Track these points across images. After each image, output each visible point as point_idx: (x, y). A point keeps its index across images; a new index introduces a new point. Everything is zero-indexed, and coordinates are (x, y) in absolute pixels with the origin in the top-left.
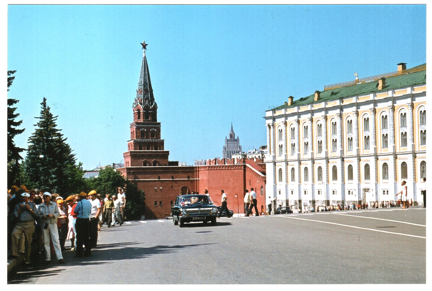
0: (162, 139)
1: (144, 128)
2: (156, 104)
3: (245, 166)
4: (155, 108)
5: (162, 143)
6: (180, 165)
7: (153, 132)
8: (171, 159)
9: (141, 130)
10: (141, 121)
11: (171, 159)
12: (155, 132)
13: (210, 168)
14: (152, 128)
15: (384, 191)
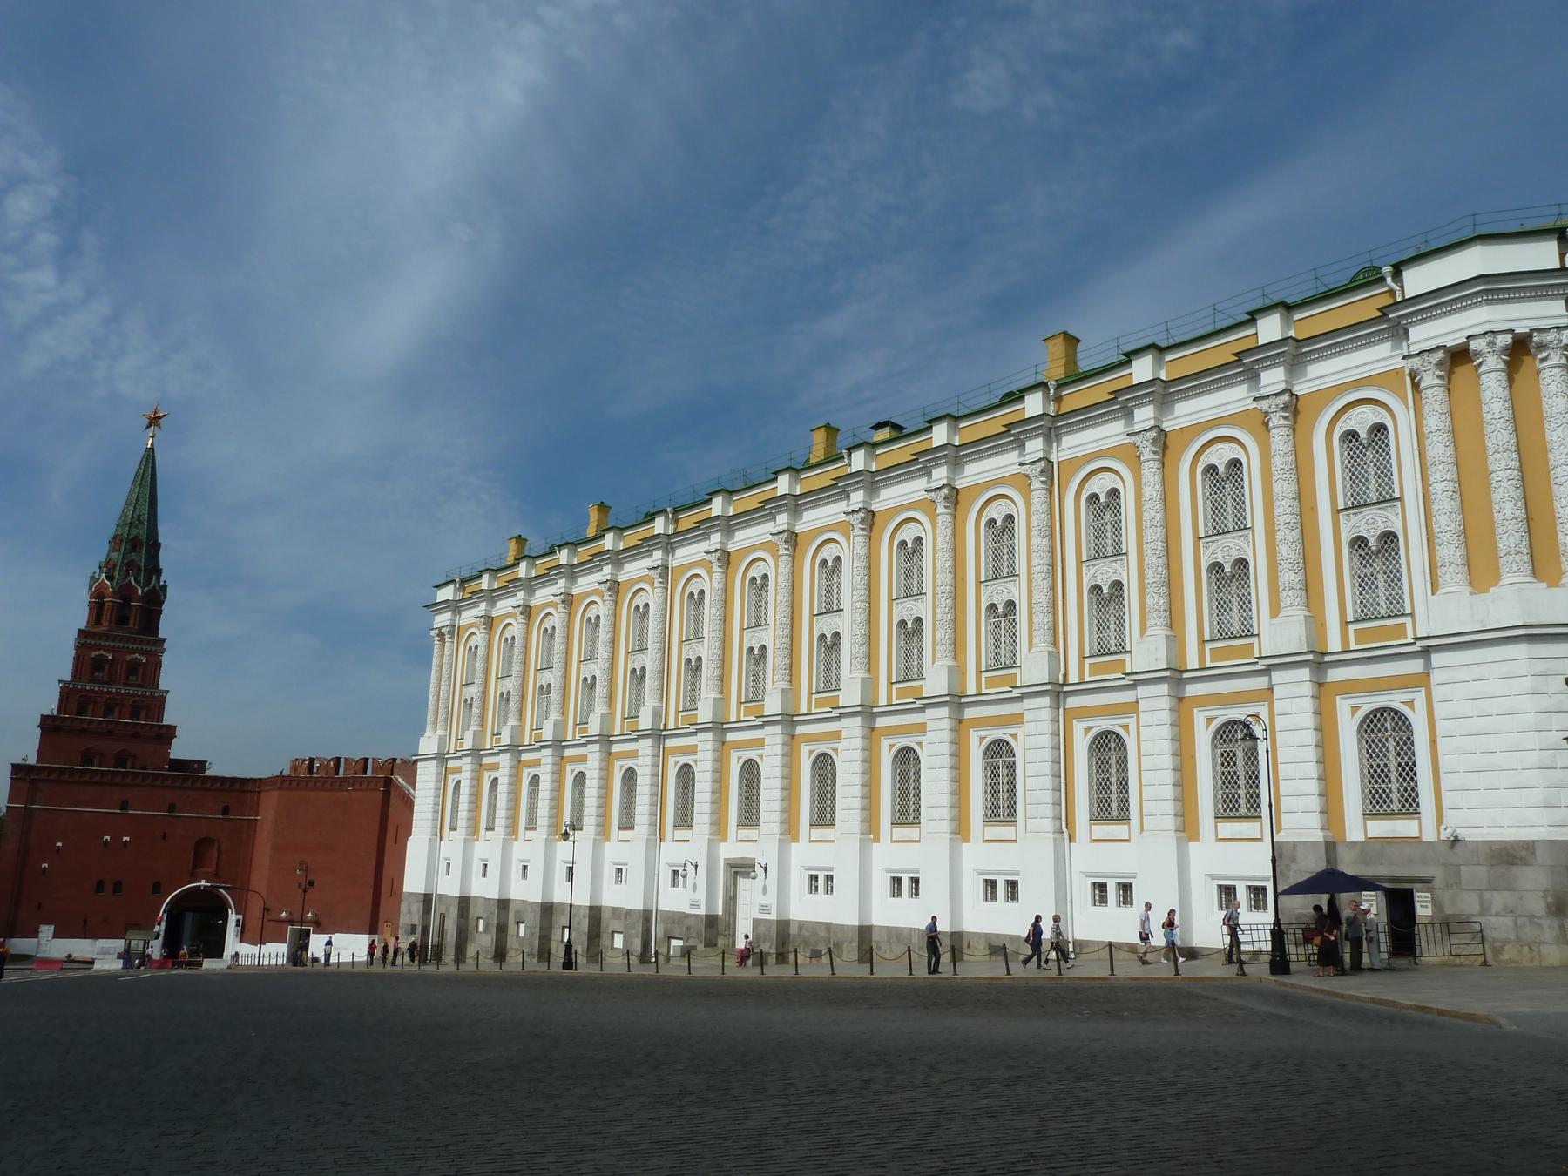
0: (162, 686)
1: (107, 649)
2: (164, 588)
3: (388, 782)
4: (156, 598)
5: (159, 703)
6: (208, 773)
7: (134, 667)
8: (179, 750)
9: (94, 654)
10: (103, 629)
11: (179, 750)
12: (140, 663)
13: (280, 782)
14: (134, 651)
15: (814, 878)
